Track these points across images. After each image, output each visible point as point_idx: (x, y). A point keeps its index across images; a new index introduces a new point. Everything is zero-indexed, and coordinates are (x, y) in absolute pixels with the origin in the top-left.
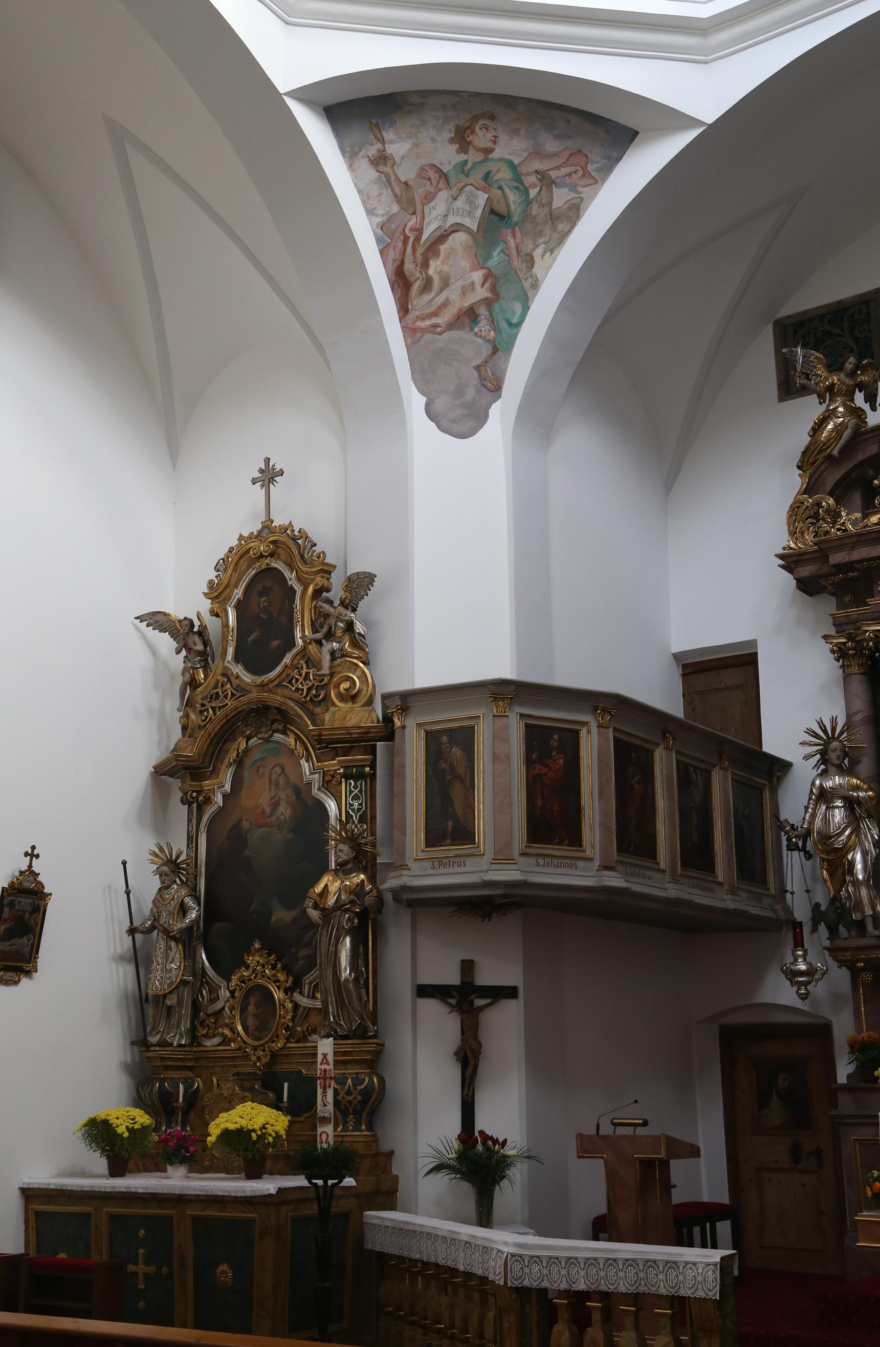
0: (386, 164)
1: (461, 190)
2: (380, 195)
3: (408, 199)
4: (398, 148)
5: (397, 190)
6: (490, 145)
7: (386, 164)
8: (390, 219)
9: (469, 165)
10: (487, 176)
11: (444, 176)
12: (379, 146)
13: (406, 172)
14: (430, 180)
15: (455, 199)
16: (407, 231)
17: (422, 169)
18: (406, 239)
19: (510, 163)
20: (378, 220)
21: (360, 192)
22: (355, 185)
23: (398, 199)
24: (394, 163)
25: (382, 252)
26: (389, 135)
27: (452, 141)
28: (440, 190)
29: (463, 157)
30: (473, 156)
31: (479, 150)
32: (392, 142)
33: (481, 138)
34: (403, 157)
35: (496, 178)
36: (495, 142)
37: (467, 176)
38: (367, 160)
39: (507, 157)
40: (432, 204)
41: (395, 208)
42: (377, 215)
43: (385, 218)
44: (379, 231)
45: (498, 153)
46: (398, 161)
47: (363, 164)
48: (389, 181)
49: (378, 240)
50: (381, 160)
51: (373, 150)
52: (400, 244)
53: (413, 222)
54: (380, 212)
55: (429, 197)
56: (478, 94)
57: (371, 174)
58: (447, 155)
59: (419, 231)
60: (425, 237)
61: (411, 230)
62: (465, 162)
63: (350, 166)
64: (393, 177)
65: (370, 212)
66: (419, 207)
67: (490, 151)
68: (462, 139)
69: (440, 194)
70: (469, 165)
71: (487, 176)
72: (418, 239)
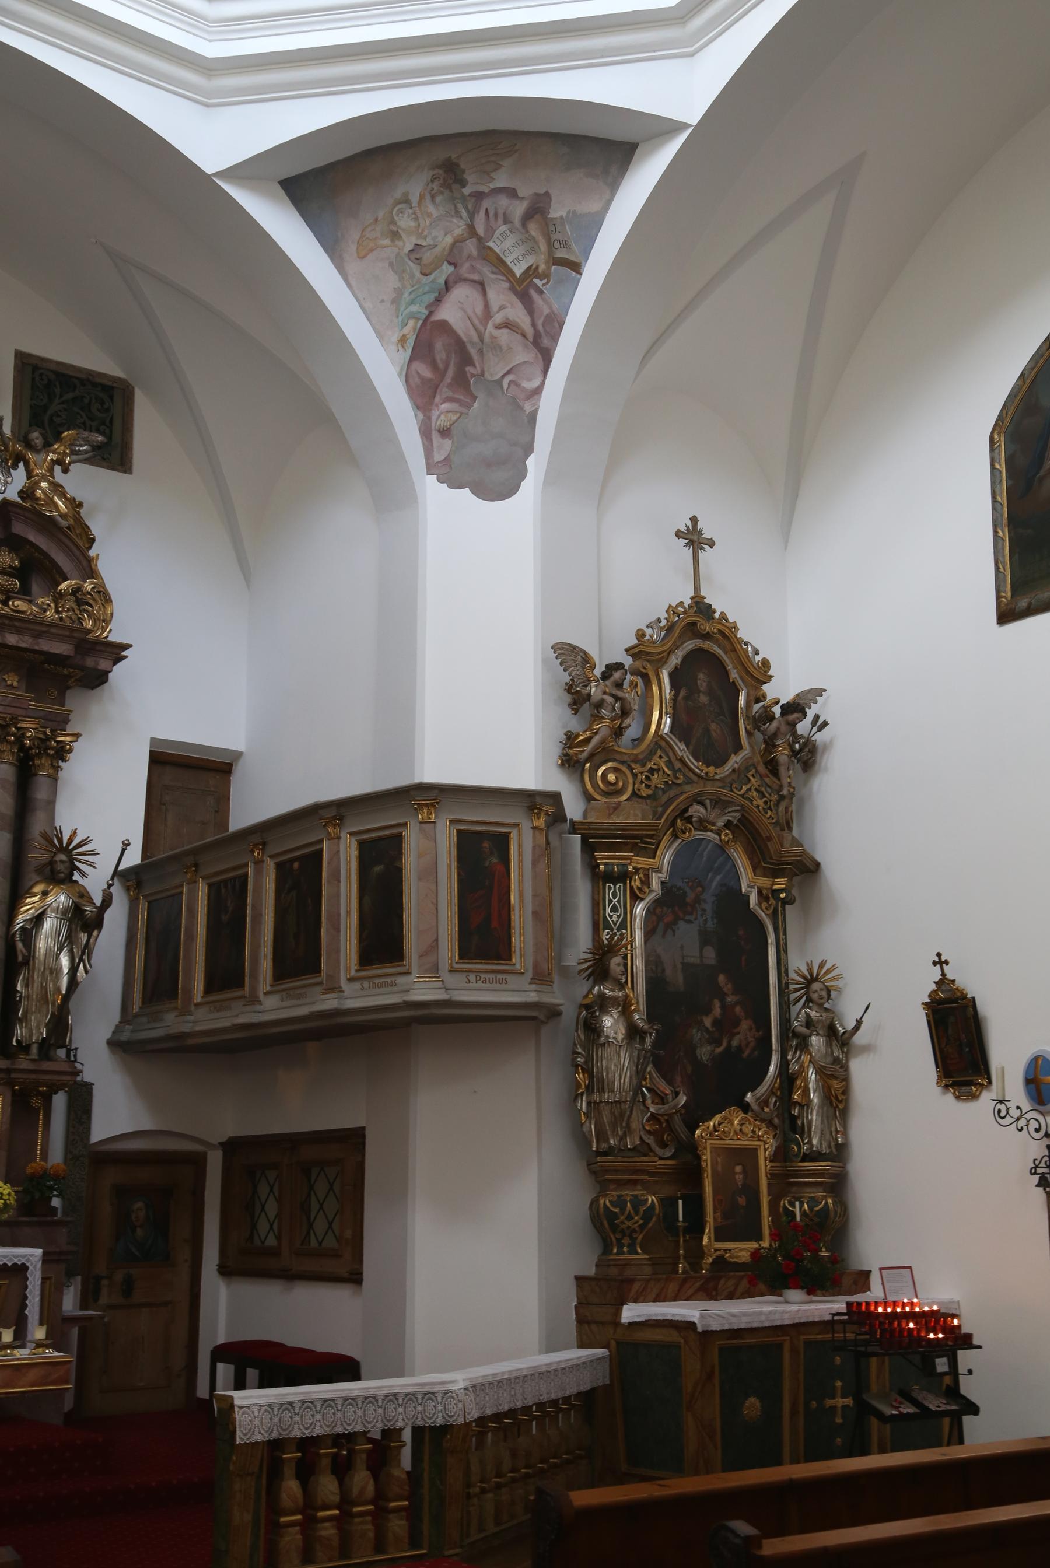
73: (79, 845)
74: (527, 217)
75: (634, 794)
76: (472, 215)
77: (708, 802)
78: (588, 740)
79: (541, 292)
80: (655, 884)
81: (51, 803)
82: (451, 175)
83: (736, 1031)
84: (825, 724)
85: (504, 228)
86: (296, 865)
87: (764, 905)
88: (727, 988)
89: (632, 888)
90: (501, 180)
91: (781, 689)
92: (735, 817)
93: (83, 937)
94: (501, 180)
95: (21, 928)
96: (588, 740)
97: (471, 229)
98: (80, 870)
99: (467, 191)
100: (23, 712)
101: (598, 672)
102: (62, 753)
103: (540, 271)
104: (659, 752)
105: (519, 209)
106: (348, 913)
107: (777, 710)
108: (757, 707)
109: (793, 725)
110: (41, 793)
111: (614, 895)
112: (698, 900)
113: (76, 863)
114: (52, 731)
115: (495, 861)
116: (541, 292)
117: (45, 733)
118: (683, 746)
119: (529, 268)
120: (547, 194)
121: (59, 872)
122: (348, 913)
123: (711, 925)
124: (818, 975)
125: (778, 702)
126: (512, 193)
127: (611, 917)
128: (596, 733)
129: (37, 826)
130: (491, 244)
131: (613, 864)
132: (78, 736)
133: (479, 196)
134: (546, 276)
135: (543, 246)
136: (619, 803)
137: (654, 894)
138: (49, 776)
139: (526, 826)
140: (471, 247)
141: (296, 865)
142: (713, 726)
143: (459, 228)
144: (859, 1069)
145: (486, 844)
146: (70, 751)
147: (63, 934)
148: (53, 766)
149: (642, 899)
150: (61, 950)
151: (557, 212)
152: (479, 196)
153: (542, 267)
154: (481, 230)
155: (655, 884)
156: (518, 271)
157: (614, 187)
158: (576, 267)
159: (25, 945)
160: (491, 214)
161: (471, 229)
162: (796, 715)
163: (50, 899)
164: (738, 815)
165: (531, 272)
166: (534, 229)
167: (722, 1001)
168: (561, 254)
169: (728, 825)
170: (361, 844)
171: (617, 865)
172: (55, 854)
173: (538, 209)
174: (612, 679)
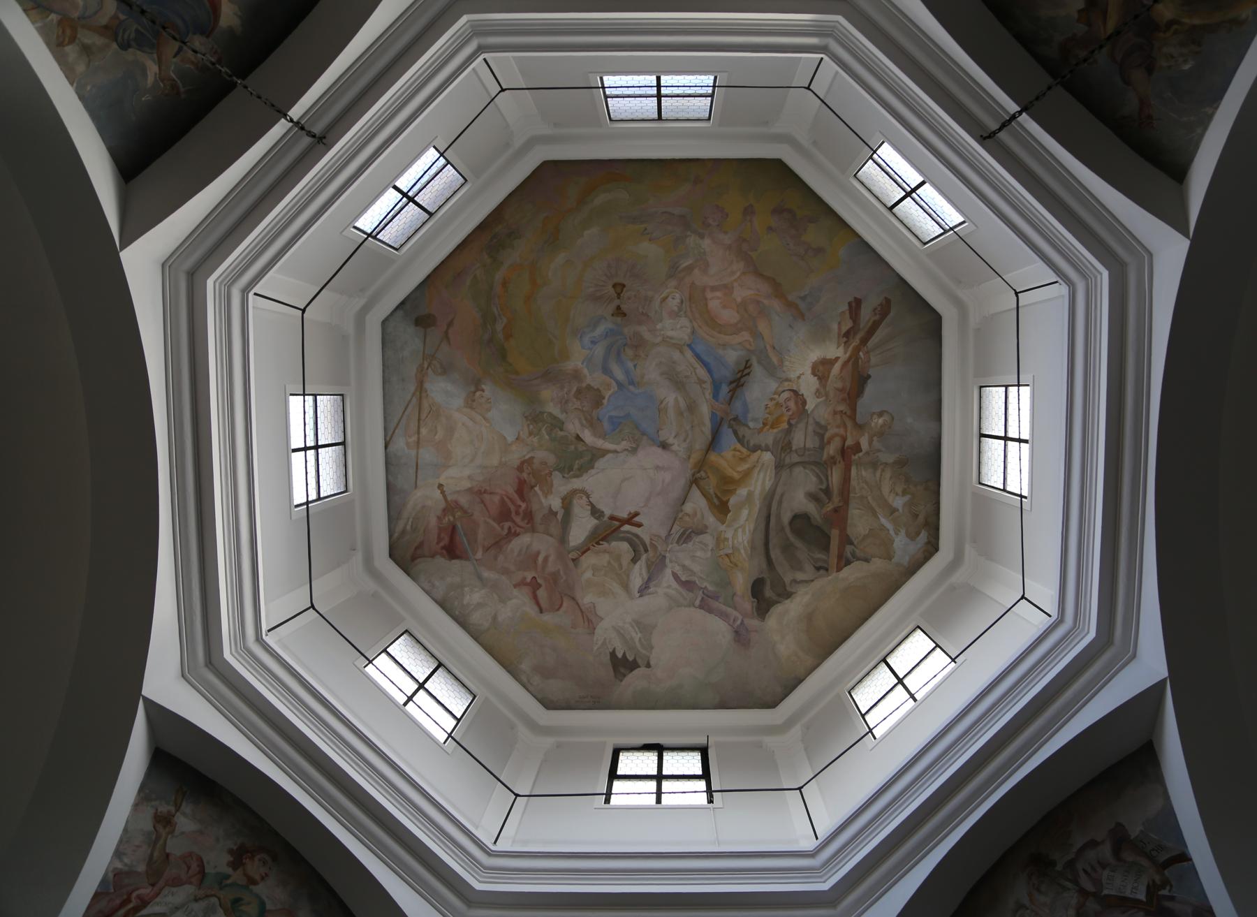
0: (165, 827)
1: (207, 896)
2: (138, 846)
3: (159, 869)
4: (185, 823)
5: (156, 854)
6: (257, 877)
7: (165, 827)
8: (130, 873)
9: (229, 882)
10: (237, 901)
11: (202, 873)
12: (173, 809)
13: (176, 847)
14: (189, 868)
15: (196, 900)
16: (134, 895)
17: (190, 854)
18: (128, 901)
19: (262, 904)
20: (119, 865)
21: (125, 830)
22: (127, 822)
23: (150, 861)
24: (172, 832)
25: (97, 896)
26: (187, 808)
27: (231, 852)
28: (191, 883)
29: (229, 871)
30: (237, 877)
31: (245, 875)
32: (184, 814)
33: (254, 867)
34: (183, 833)
35: (243, 908)
36: (263, 878)
37: (221, 889)
38: (152, 811)
39: (264, 898)
40: (174, 890)
41: (141, 868)
42: (121, 861)
43: (126, 869)
44: (111, 875)
45: (260, 889)
46: (177, 832)
47: (148, 812)
48: (155, 843)
49: (104, 882)
50: (163, 821)
51: (164, 808)
52: (118, 902)
53: (145, 891)
54: (126, 860)
55: (176, 882)
56: (277, 834)
57: (147, 824)
58: (218, 861)
59: (144, 903)
60: (144, 912)
61: (139, 897)
62: (228, 877)
63: (136, 806)
64: (161, 842)
65: (118, 854)
66: (161, 883)
67: (254, 882)
68: (239, 858)
69: (187, 887)
70: (229, 882)
71: (237, 901)
72: (137, 909)
74: (1117, 851)
76: (1075, 881)
79: (1172, 898)
82: (1040, 866)
85: (1106, 873)
90: (1078, 841)
94: (1078, 841)
97: (1083, 892)
99: (1059, 867)
103: (1158, 883)
105: (1106, 851)
116: (1172, 898)
119: (1148, 887)
120: (1119, 825)
126: (1093, 844)
130: (1106, 892)
133: (1071, 864)
134: (1166, 883)
135: (1145, 862)
140: (1092, 905)
143: (1073, 898)
151: (1135, 831)
152: (1071, 864)
153: (1157, 878)
154: (1089, 887)
156: (1142, 896)
157: (1159, 780)
158: (1184, 857)
160: (1089, 870)
161: (1083, 892)
165: (1152, 890)
166: (1128, 856)
168: (1163, 857)
173: (1120, 840)
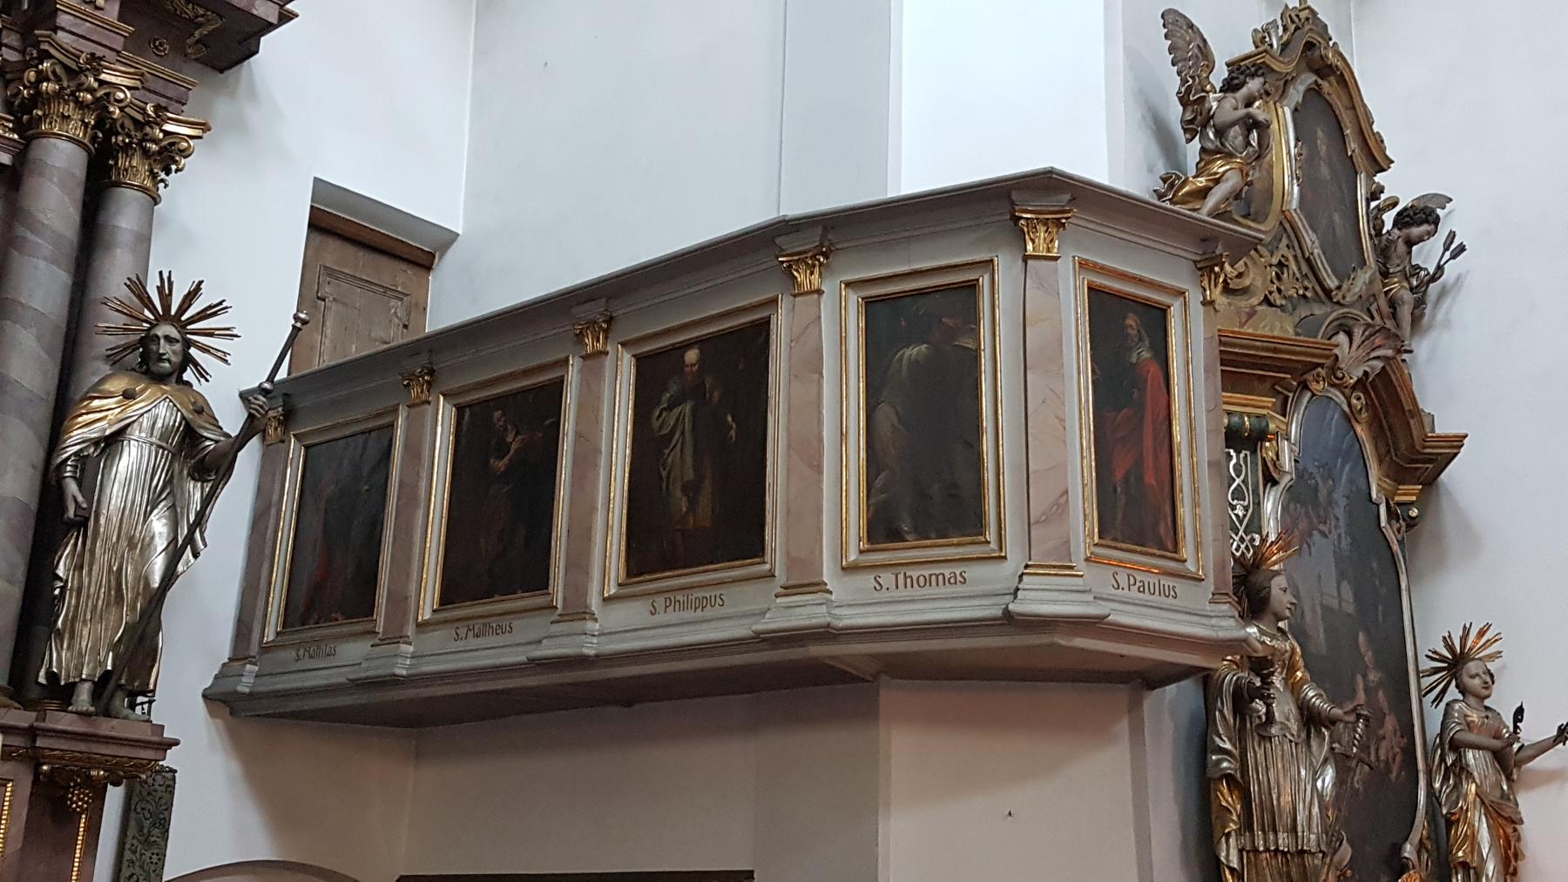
73: (203, 315)
75: (1267, 301)
77: (1358, 333)
78: (1203, 193)
80: (1287, 462)
81: (143, 241)
83: (1381, 732)
84: (1462, 248)
86: (692, 356)
87: (1396, 526)
88: (1369, 657)
89: (1264, 459)
91: (1401, 185)
92: (1373, 368)
93: (195, 492)
95: (75, 454)
96: (1203, 193)
98: (196, 364)
100: (110, 55)
101: (1219, 75)
102: (168, 157)
104: (1285, 241)
106: (843, 436)
107: (1389, 218)
108: (1373, 204)
109: (1410, 243)
110: (125, 213)
111: (1238, 468)
112: (1331, 502)
113: (192, 351)
114: (158, 108)
115: (1146, 355)
117: (144, 110)
118: (1314, 237)
121: (160, 358)
122: (843, 436)
123: (1345, 543)
124: (1463, 646)
125: (1395, 204)
127: (1234, 508)
128: (1217, 181)
129: (113, 279)
131: (1242, 413)
132: (205, 127)
136: (1252, 307)
137: (1287, 478)
138: (143, 189)
139: (1195, 297)
141: (692, 356)
142: (1337, 217)
144: (1528, 804)
145: (1131, 321)
146: (185, 153)
147: (159, 479)
148: (153, 176)
149: (1275, 483)
150: (153, 504)
155: (1287, 462)
159: (80, 485)
162: (1425, 228)
163: (137, 407)
164: (1379, 364)
167: (1365, 676)
169: (1361, 384)
170: (870, 304)
171: (1249, 415)
172: (153, 326)
174: (1244, 90)
